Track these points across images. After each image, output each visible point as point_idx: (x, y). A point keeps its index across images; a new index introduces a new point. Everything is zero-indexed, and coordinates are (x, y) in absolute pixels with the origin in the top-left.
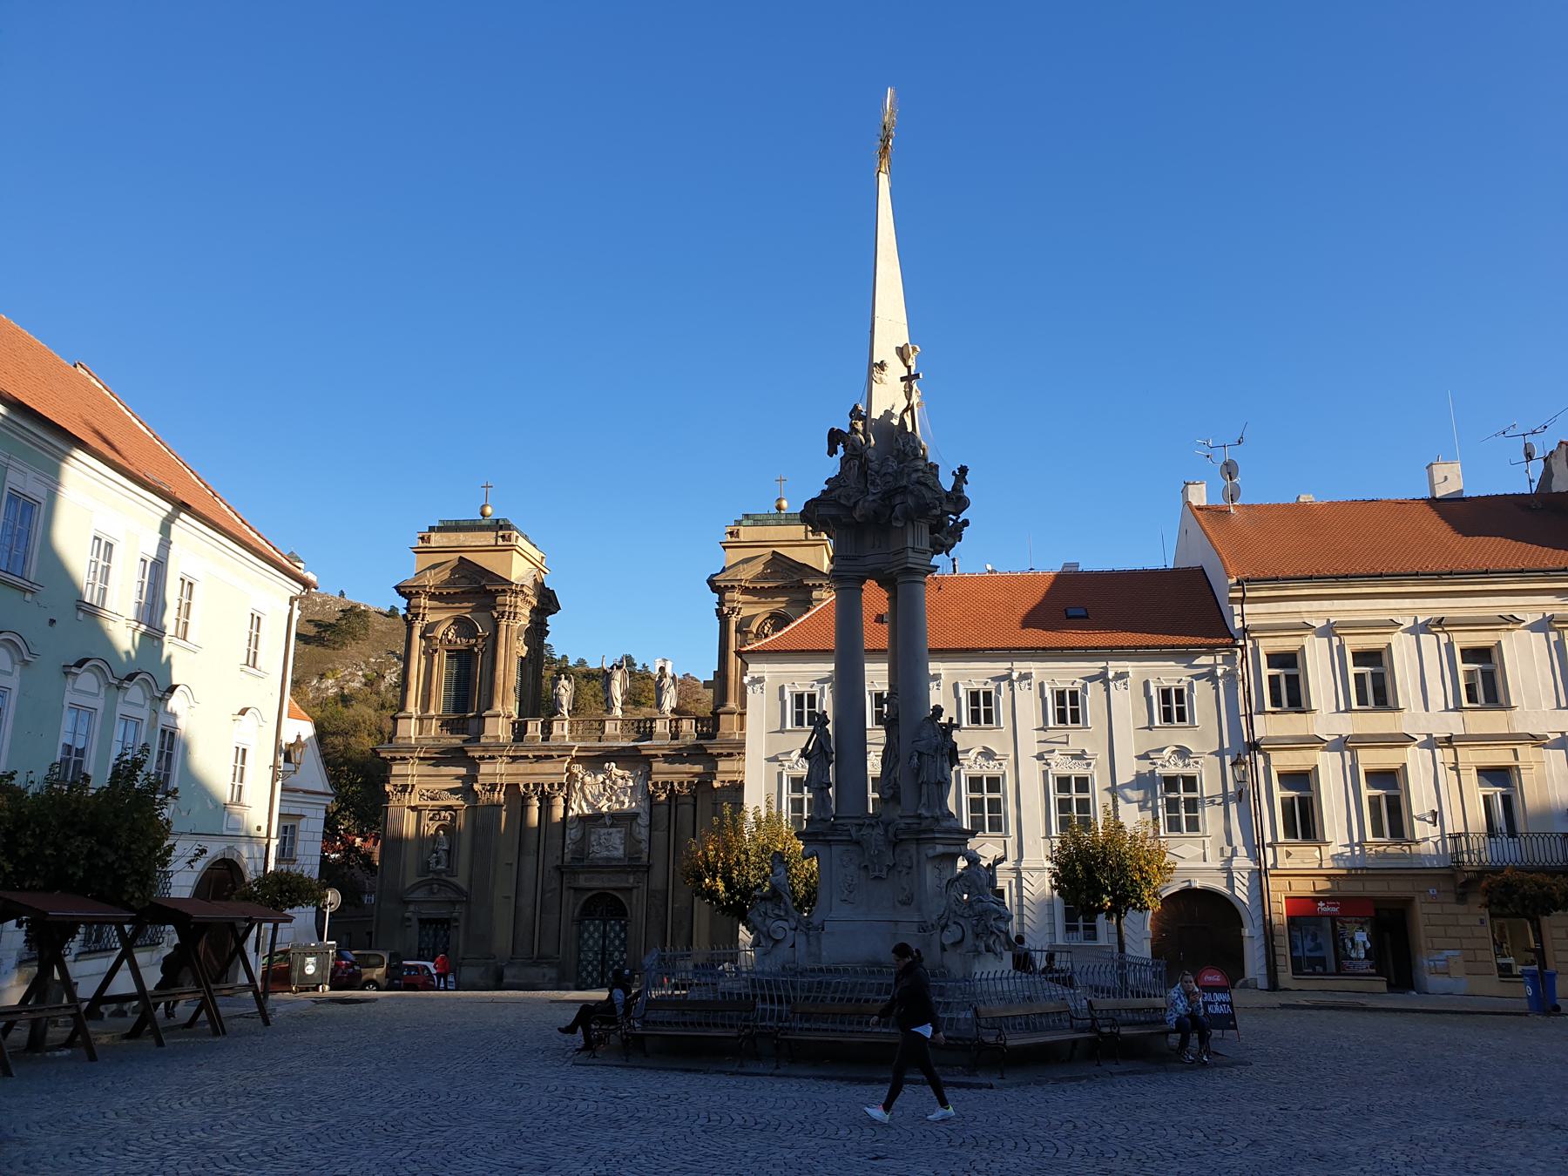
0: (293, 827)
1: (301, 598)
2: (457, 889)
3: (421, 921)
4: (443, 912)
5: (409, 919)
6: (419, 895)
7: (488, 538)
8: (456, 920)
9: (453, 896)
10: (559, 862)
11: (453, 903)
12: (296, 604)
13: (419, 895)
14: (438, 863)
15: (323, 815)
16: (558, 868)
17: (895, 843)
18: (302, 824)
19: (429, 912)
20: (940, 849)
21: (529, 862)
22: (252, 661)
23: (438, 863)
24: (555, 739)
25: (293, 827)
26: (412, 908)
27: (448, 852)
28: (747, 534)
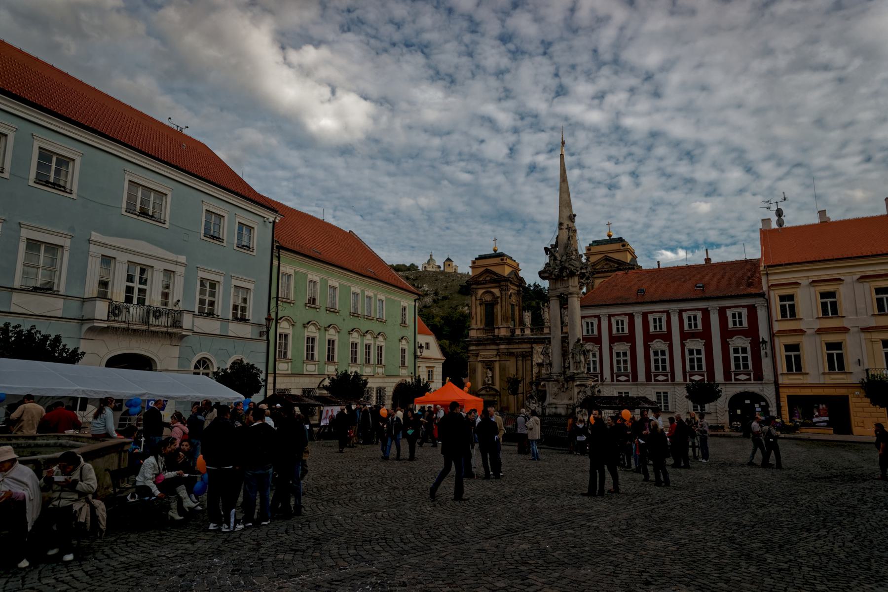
2: (496, 390)
4: (491, 398)
6: (483, 392)
9: (494, 393)
13: (483, 392)
17: (567, 382)
20: (578, 383)
22: (404, 322)
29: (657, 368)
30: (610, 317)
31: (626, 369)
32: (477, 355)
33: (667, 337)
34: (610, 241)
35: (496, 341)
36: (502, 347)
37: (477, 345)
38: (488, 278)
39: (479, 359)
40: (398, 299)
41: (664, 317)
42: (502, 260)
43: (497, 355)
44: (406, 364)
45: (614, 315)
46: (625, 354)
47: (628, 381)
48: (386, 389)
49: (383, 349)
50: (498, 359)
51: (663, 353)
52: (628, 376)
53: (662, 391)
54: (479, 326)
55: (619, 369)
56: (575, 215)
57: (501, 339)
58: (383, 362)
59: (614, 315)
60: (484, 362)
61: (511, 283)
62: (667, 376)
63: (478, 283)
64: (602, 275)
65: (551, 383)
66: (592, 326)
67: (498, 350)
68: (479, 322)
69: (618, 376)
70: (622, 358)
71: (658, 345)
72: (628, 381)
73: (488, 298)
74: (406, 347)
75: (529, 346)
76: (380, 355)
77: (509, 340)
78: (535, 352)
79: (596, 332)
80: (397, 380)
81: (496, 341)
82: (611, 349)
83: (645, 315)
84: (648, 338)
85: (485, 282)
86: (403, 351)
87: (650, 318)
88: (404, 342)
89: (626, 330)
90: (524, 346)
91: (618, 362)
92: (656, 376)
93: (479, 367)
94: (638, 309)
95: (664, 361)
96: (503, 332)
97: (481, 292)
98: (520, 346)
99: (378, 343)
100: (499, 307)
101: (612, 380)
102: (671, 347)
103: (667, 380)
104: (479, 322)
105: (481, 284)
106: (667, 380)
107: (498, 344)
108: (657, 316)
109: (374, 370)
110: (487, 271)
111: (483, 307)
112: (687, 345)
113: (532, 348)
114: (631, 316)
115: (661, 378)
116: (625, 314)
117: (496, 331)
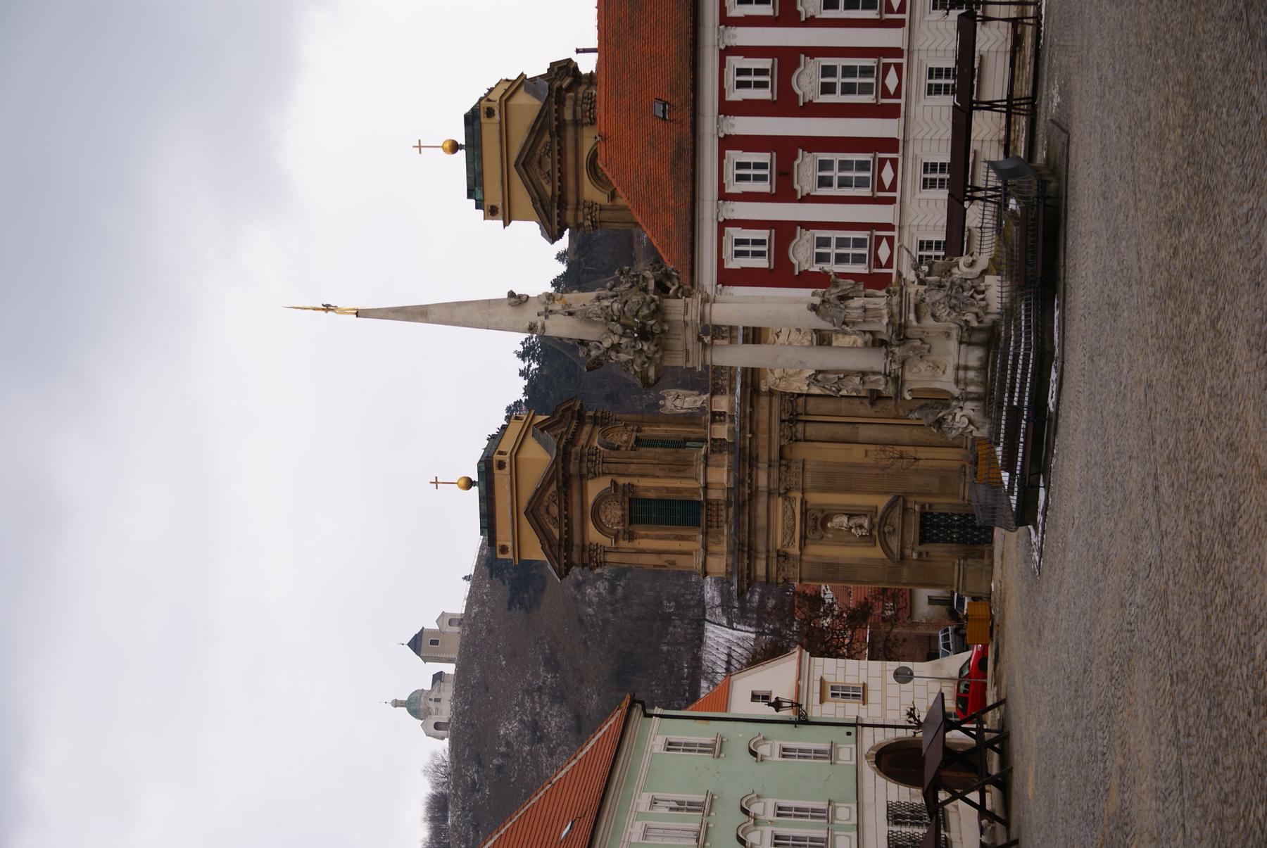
0: (833, 688)
1: (644, 709)
2: (891, 506)
3: (923, 540)
4: (914, 520)
5: (920, 554)
6: (895, 544)
7: (502, 479)
8: (923, 506)
9: (898, 510)
10: (866, 402)
11: (905, 510)
12: (649, 711)
13: (895, 544)
14: (861, 527)
15: (819, 660)
16: (872, 403)
18: (830, 679)
19: (913, 534)
20: (912, 317)
21: (865, 433)
23: (861, 527)
24: (732, 409)
25: (833, 688)
26: (908, 552)
27: (850, 516)
28: (494, 195)
29: (866, 89)
30: (724, 196)
31: (863, 166)
32: (784, 556)
33: (788, 58)
34: (473, 145)
35: (743, 498)
36: (762, 480)
37: (752, 553)
38: (555, 510)
39: (795, 550)
40: (646, 759)
41: (736, 62)
42: (501, 465)
43: (785, 495)
44: (825, 746)
45: (721, 186)
46: (825, 165)
47: (894, 163)
48: (893, 798)
49: (783, 803)
50: (798, 496)
51: (828, 71)
52: (882, 163)
53: (925, 81)
54: (695, 545)
55: (861, 183)
56: (512, 294)
57: (740, 482)
58: (822, 805)
59: (721, 186)
60: (804, 537)
61: (572, 442)
62: (886, 68)
63: (567, 544)
64: (571, 181)
65: (908, 376)
66: (745, 242)
67: (770, 493)
68: (685, 546)
69: (881, 187)
70: (835, 174)
71: (807, 82)
72: (894, 163)
73: (613, 514)
74: (777, 745)
75: (764, 401)
76: (800, 812)
77: (745, 459)
78: (782, 386)
79: (763, 234)
80: (869, 771)
81: (743, 498)
82: (808, 199)
83: (728, 109)
84: (786, 104)
85: (566, 521)
86: (786, 752)
87: (736, 95)
88: (763, 750)
89: (764, 157)
90: (763, 415)
91: (844, 183)
92: (886, 93)
93: (821, 551)
94: (712, 126)
95: (848, 71)
96: (720, 476)
97: (594, 535)
98: (763, 426)
99: (770, 815)
100: (642, 483)
101: (891, 201)
102: (813, 52)
103: (899, 68)
104: (685, 546)
105: (569, 532)
106: (899, 68)
107: (754, 494)
108: (731, 78)
109: (843, 828)
110: (533, 512)
111: (640, 530)
112: (811, 12)
113: (771, 393)
114: (728, 142)
115: (891, 81)
116: (721, 157)
117: (714, 495)
